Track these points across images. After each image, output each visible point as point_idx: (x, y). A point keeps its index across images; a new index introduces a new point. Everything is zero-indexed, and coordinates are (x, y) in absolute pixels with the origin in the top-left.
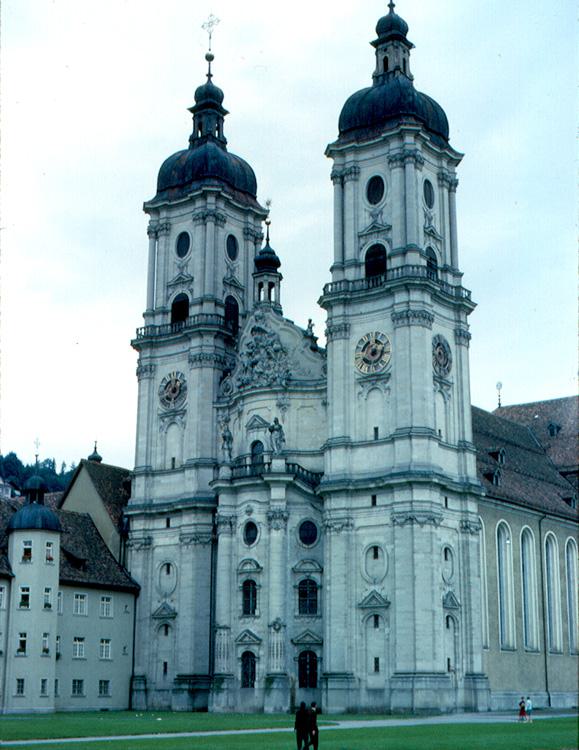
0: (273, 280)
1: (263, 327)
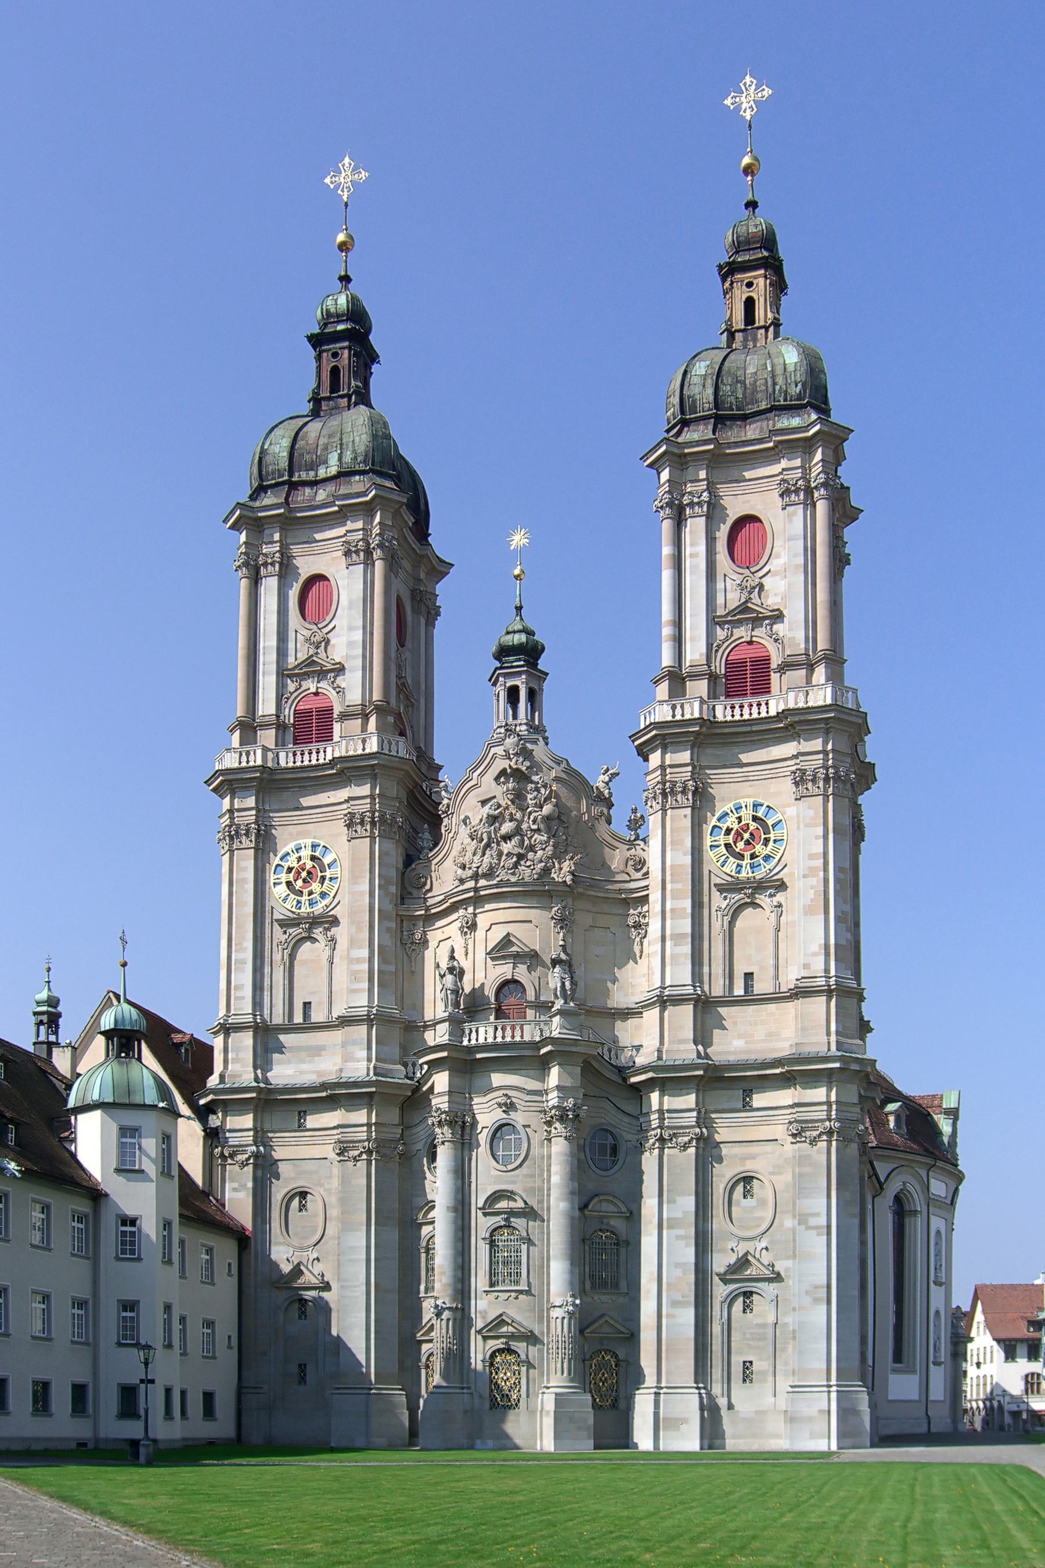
1: (524, 769)
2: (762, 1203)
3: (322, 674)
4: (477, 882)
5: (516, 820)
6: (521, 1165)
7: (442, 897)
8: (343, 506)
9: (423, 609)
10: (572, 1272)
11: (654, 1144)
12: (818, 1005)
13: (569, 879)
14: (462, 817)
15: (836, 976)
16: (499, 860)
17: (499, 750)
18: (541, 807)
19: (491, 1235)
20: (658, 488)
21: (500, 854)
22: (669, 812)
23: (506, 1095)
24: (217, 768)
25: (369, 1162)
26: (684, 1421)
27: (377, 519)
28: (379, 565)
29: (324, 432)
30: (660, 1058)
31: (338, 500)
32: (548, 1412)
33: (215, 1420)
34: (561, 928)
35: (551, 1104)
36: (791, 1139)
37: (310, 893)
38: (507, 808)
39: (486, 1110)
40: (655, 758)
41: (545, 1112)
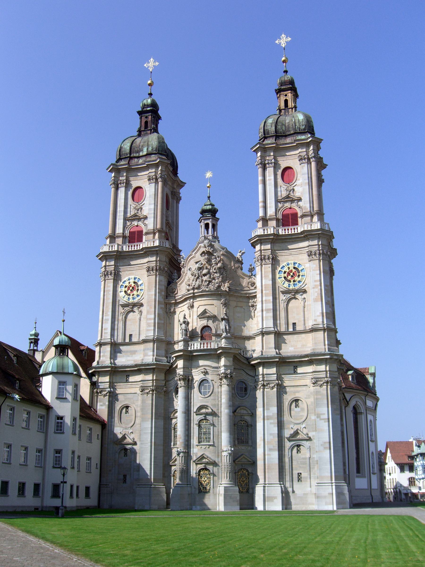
0: (215, 223)
1: (211, 251)
2: (303, 410)
3: (139, 219)
4: (194, 290)
5: (208, 269)
6: (210, 395)
7: (181, 296)
8: (148, 164)
9: (175, 198)
10: (230, 437)
11: (261, 387)
12: (320, 335)
13: (227, 289)
14: (189, 268)
15: (326, 324)
16: (202, 283)
17: (202, 245)
18: (217, 264)
19: (199, 423)
20: (257, 158)
21: (202, 281)
22: (263, 266)
23: (205, 369)
24: (101, 251)
25: (153, 394)
26: (275, 498)
27: (160, 168)
28: (160, 184)
29: (142, 141)
30: (262, 354)
31: (146, 162)
32: (221, 494)
33: (90, 498)
34: (225, 307)
35: (221, 372)
36: (312, 385)
37: (133, 295)
38: (205, 265)
39: (197, 374)
40: (258, 247)
41: (219, 375)
